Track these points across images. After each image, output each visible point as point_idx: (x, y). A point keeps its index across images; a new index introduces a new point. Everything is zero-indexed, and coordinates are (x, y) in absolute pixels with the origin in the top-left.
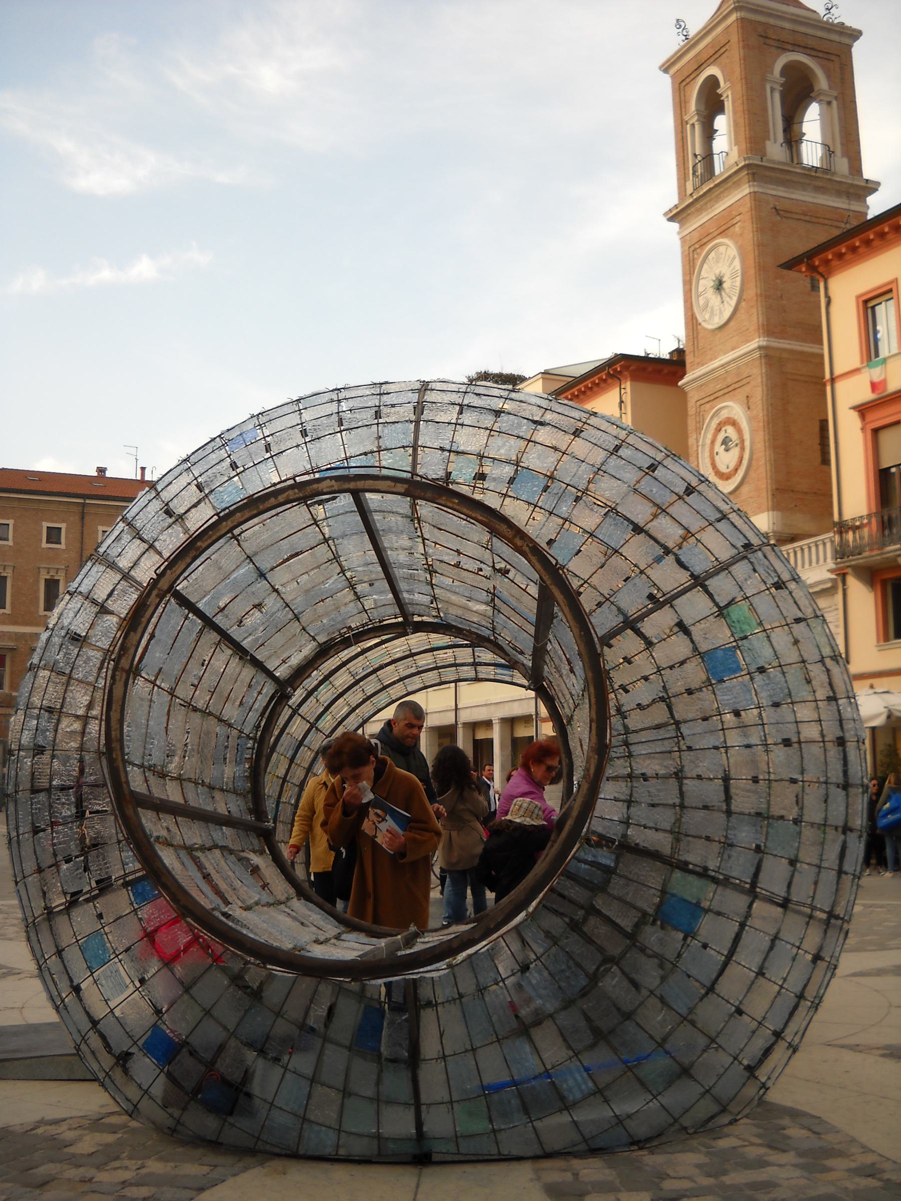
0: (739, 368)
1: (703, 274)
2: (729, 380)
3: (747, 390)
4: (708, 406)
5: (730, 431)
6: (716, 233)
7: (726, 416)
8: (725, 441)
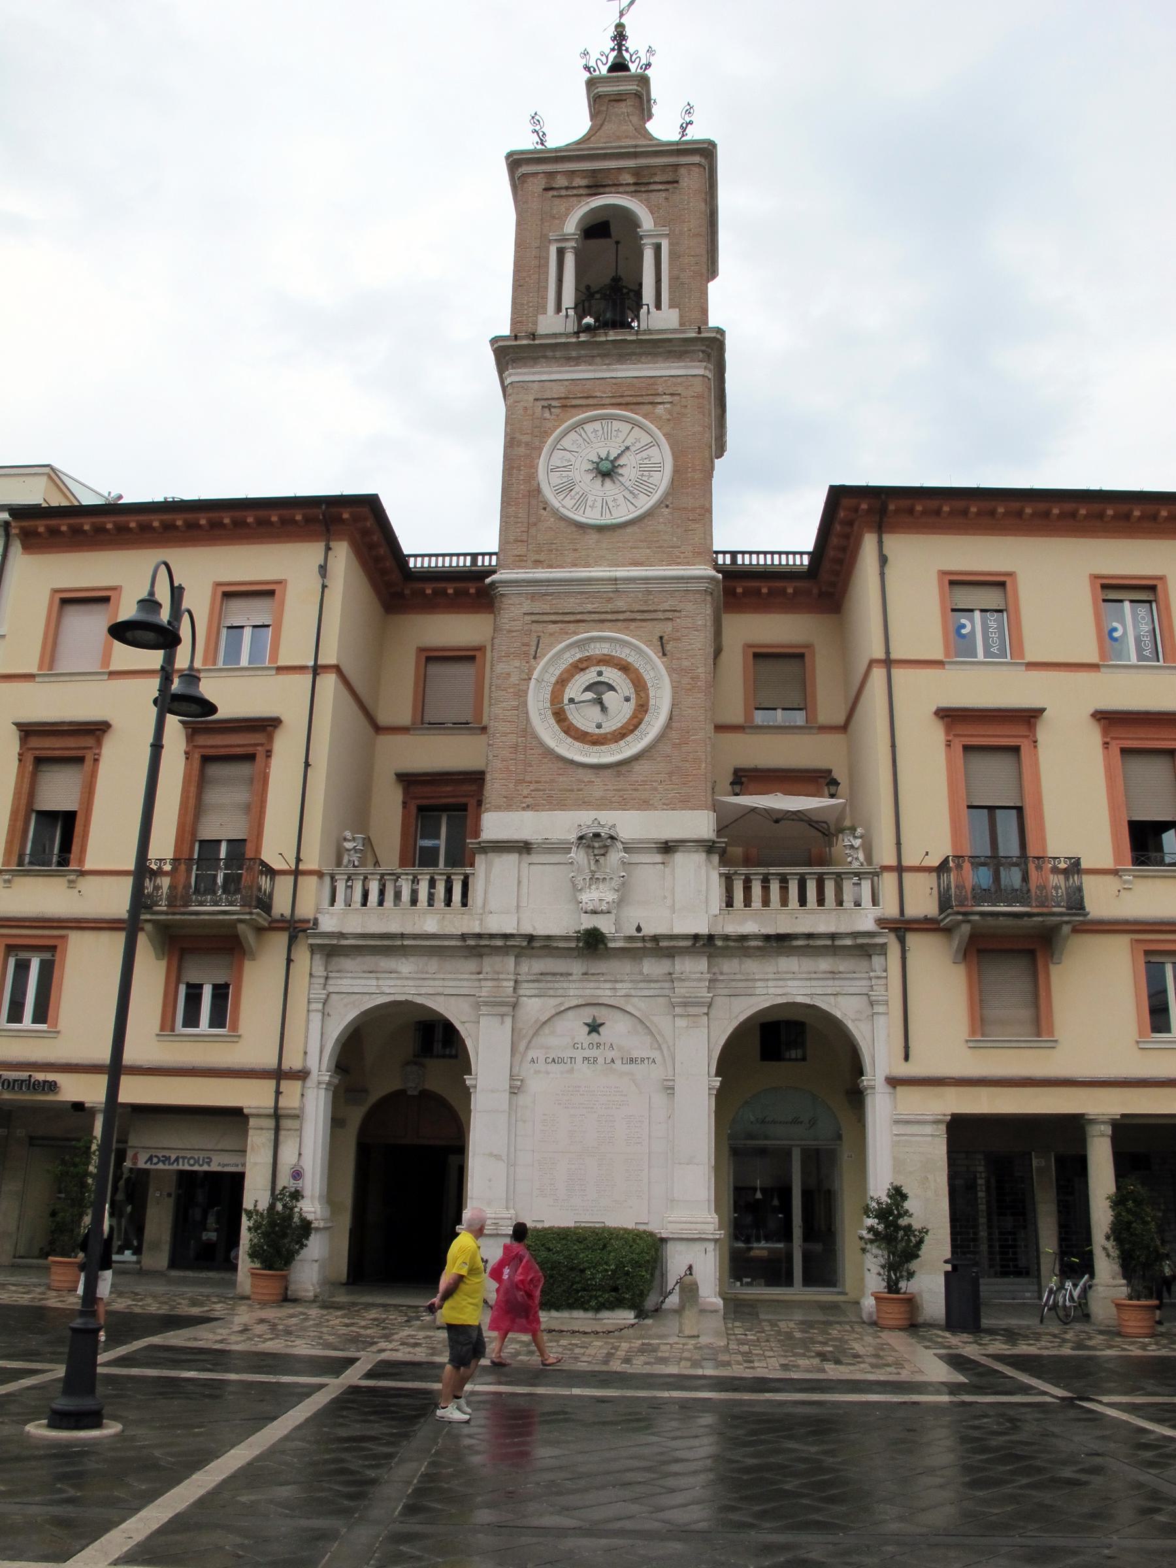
0: (649, 592)
1: (566, 442)
2: (621, 604)
3: (668, 628)
4: (552, 628)
5: (611, 675)
6: (608, 401)
7: (605, 652)
8: (599, 688)
